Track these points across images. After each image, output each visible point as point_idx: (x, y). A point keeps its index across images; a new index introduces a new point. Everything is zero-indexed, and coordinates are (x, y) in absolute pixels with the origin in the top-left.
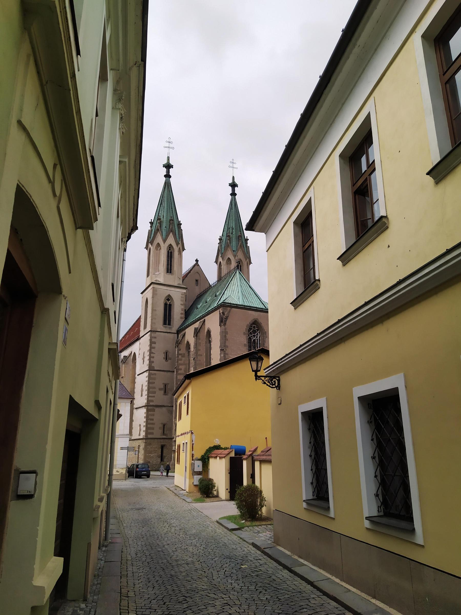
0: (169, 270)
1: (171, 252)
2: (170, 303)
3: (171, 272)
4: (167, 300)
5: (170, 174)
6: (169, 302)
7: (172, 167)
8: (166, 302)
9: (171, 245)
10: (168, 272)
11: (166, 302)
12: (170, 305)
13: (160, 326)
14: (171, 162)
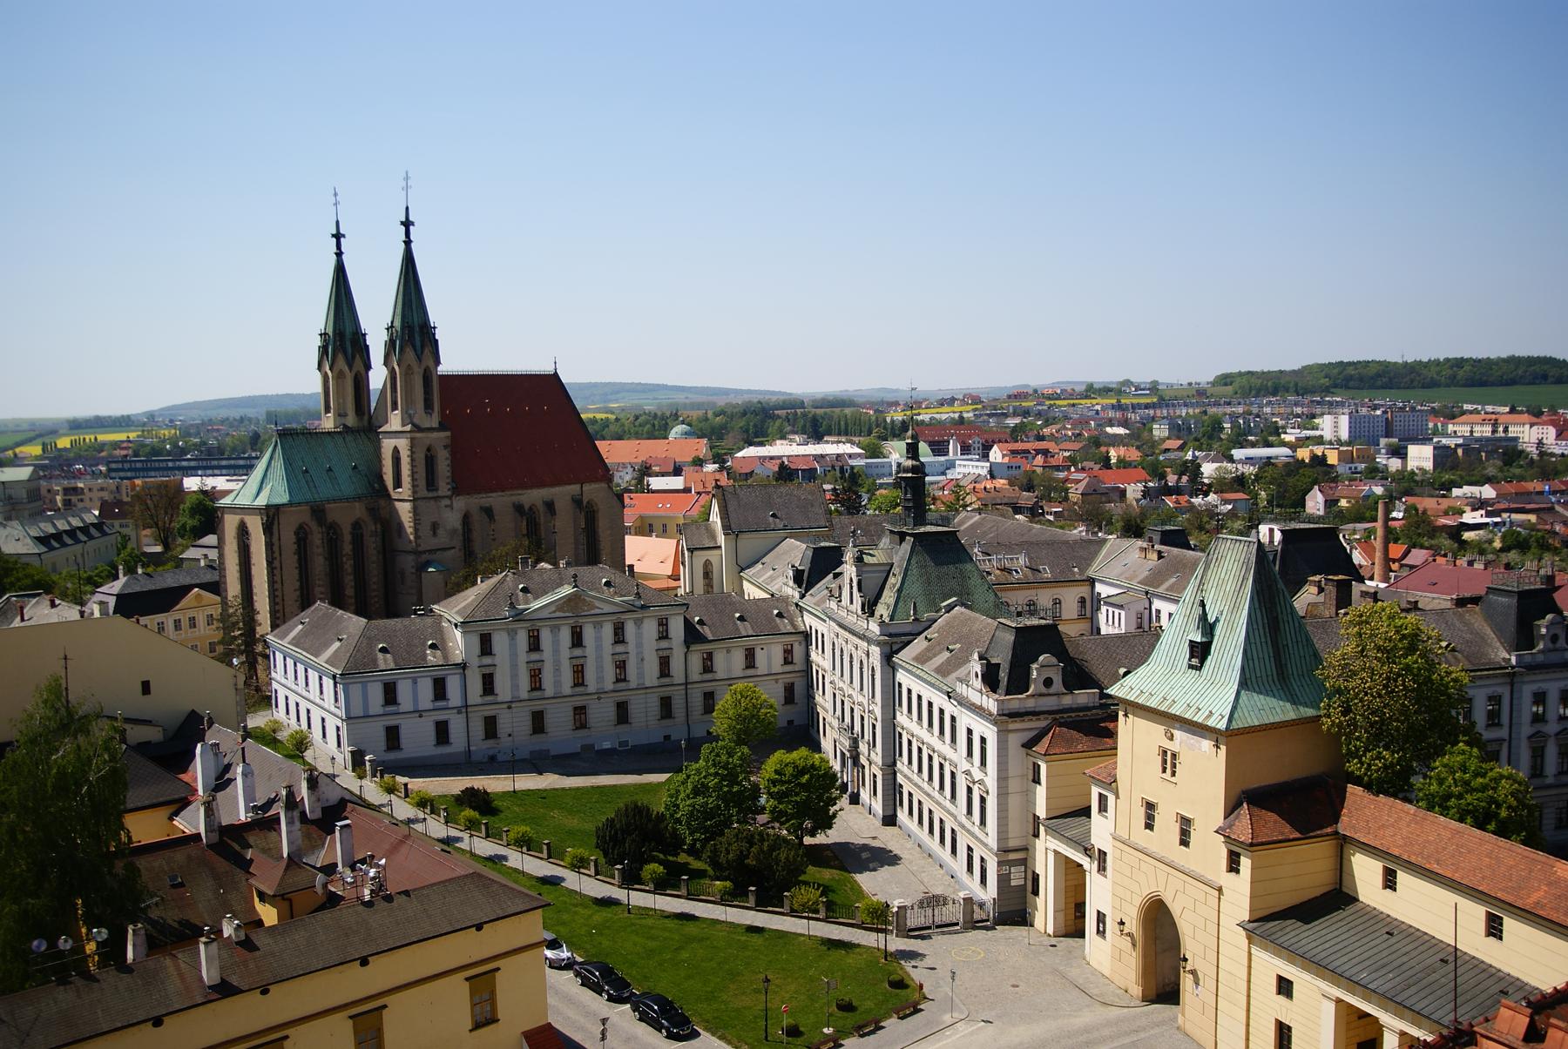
7: (344, 236)
13: (423, 492)
14: (342, 232)
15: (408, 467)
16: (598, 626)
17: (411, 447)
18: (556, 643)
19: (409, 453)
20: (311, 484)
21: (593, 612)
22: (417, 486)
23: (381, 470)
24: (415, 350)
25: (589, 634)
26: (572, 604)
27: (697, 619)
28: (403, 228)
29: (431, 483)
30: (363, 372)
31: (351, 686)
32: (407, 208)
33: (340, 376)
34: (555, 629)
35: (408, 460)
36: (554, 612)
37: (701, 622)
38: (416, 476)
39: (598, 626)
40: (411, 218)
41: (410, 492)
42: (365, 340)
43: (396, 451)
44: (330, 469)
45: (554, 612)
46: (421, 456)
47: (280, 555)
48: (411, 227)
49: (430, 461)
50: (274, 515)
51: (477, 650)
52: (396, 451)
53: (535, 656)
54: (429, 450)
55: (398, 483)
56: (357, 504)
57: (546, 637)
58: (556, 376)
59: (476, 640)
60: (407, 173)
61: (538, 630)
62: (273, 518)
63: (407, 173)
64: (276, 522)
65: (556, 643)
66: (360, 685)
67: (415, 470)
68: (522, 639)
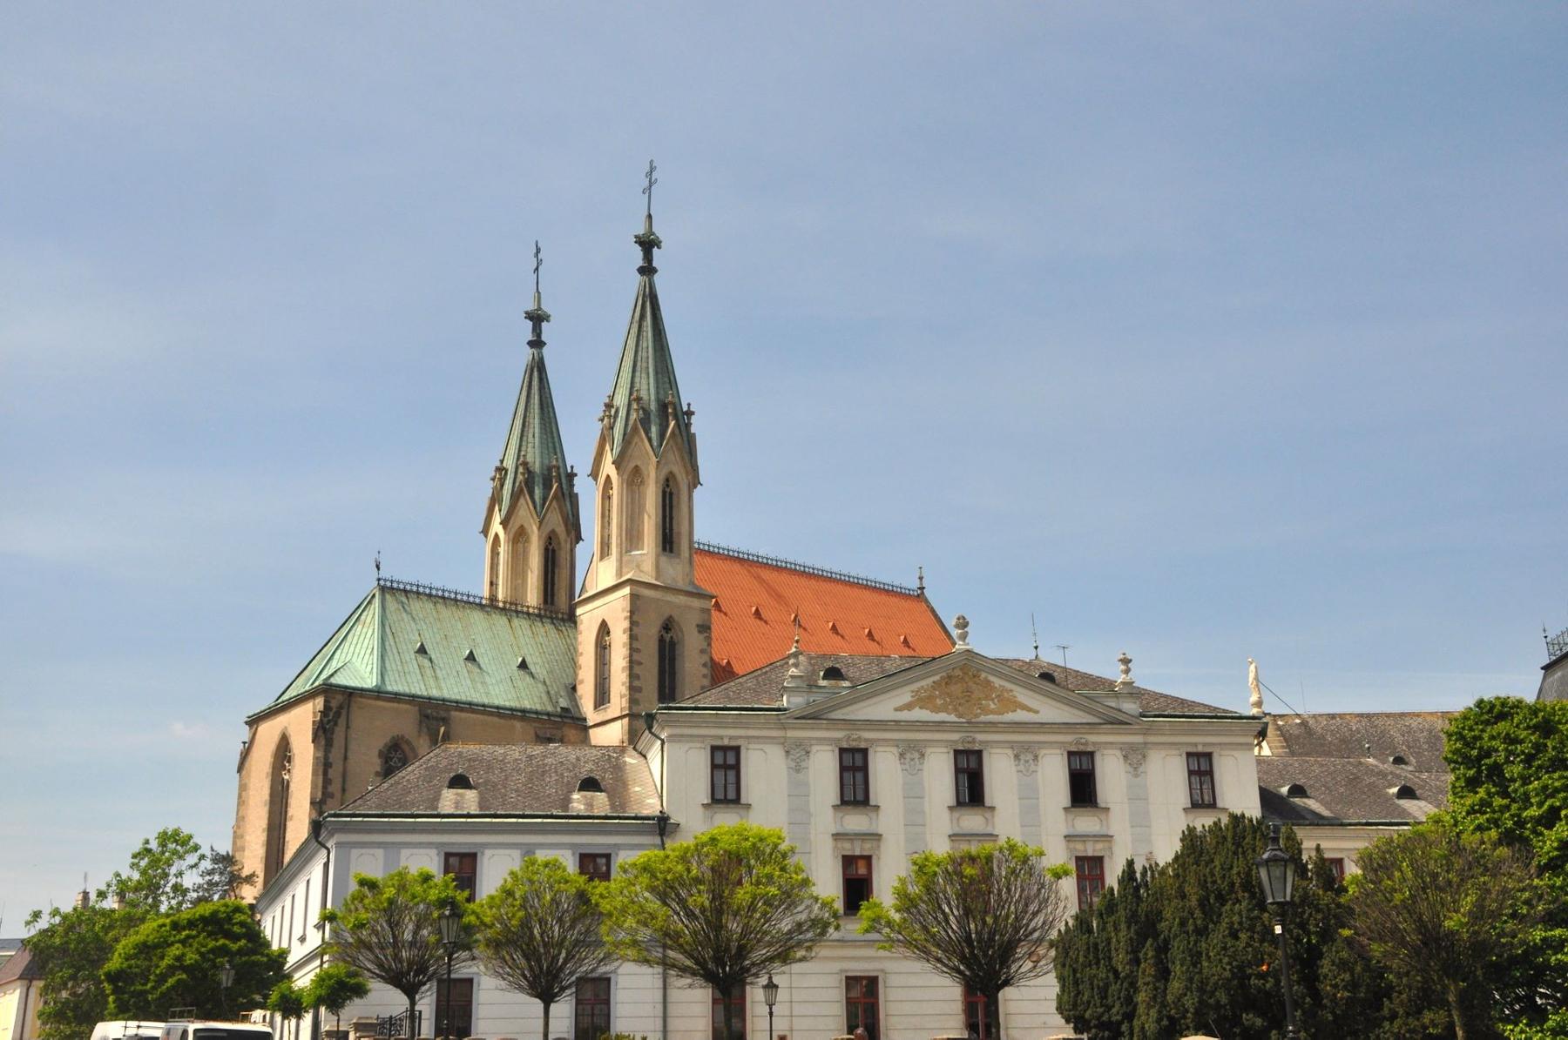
0: (668, 542)
1: (554, 551)
2: (672, 637)
3: (671, 551)
4: (664, 628)
5: (544, 338)
6: (669, 635)
7: (546, 318)
8: (662, 636)
9: (553, 531)
10: (664, 549)
11: (662, 636)
12: (673, 644)
15: (625, 651)
16: (1025, 753)
17: (632, 612)
18: (914, 796)
19: (626, 624)
20: (429, 672)
21: (1010, 717)
22: (639, 690)
23: (576, 674)
24: (650, 440)
25: (999, 772)
26: (956, 689)
27: (1285, 790)
28: (638, 252)
29: (668, 689)
30: (561, 530)
31: (355, 852)
32: (650, 216)
33: (519, 537)
34: (912, 752)
35: (625, 638)
36: (909, 707)
37: (1298, 790)
38: (637, 670)
39: (1025, 753)
40: (659, 231)
41: (625, 703)
42: (571, 485)
43: (604, 629)
44: (471, 658)
45: (909, 707)
46: (652, 631)
47: (344, 790)
48: (655, 250)
49: (668, 653)
50: (341, 707)
51: (701, 790)
52: (604, 629)
53: (856, 821)
54: (667, 626)
55: (602, 698)
56: (518, 725)
57: (885, 770)
58: (920, 596)
59: (698, 763)
60: (651, 162)
61: (865, 752)
62: (338, 714)
63: (651, 162)
64: (342, 721)
65: (914, 796)
66: (380, 852)
67: (636, 657)
68: (824, 768)
